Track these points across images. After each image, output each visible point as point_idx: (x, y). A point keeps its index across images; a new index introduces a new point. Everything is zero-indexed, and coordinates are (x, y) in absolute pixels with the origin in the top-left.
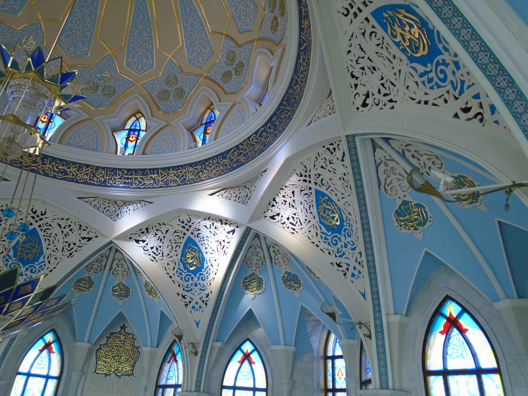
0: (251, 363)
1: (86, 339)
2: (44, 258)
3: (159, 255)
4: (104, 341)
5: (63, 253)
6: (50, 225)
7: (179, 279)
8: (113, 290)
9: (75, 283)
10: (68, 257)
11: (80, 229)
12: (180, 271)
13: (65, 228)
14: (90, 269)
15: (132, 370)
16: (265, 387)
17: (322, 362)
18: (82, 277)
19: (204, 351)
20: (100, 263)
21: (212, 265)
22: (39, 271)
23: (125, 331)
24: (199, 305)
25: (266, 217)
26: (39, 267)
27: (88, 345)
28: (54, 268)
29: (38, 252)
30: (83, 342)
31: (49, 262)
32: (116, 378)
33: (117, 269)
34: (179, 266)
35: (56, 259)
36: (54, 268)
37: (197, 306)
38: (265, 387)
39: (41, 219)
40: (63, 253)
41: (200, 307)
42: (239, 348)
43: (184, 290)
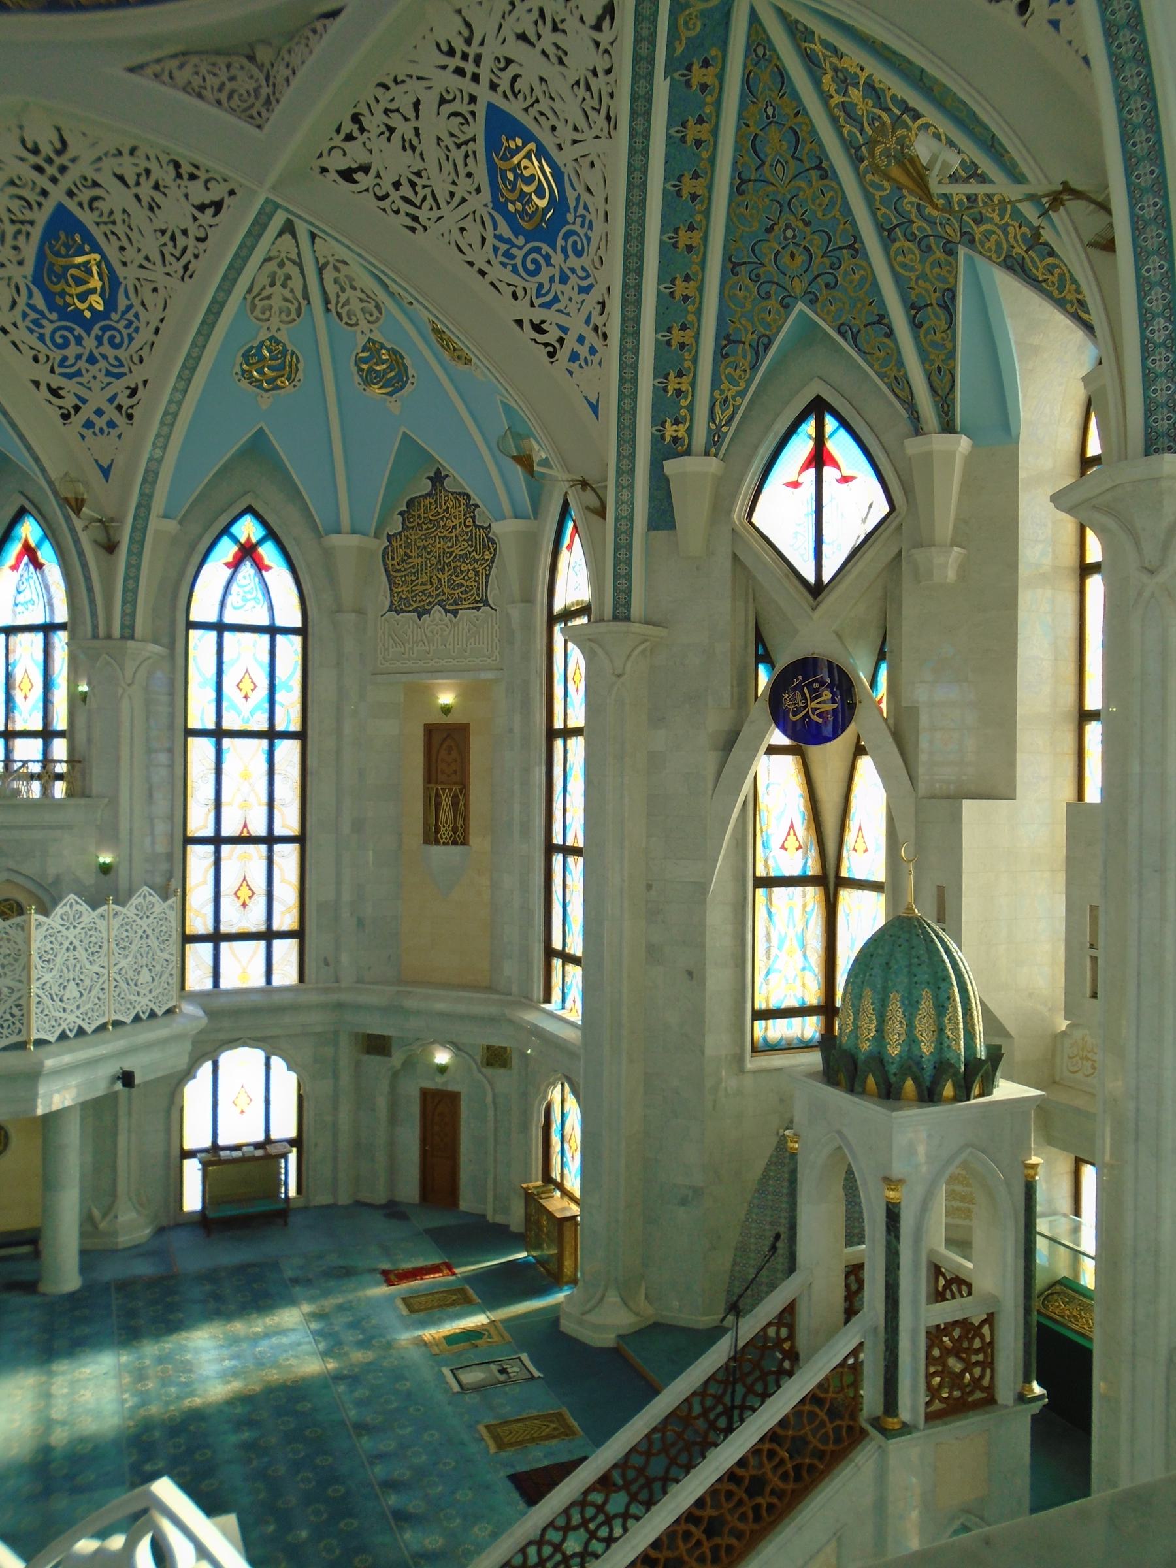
2: (128, 297)
3: (426, 206)
5: (168, 269)
6: (96, 184)
7: (507, 275)
10: (183, 279)
11: (179, 176)
12: (503, 247)
13: (138, 184)
21: (588, 190)
22: (131, 339)
24: (587, 344)
26: (127, 327)
27: (354, 540)
28: (162, 320)
30: (339, 532)
32: (446, 619)
34: (495, 227)
35: (155, 290)
36: (162, 320)
39: (63, 169)
40: (168, 269)
43: (532, 305)
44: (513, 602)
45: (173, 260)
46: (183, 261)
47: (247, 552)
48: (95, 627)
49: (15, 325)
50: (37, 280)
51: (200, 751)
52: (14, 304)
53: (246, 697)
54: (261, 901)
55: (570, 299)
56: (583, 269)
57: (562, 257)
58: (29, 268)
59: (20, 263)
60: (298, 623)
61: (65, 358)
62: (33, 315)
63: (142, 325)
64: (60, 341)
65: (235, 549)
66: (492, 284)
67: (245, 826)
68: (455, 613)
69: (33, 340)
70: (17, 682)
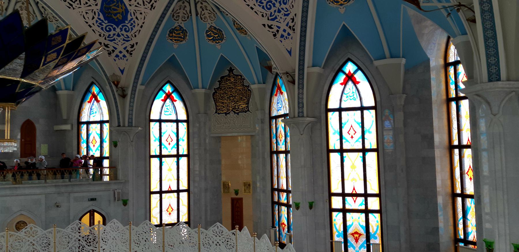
1: (200, 85)
2: (131, 16)
4: (217, 85)
8: (208, 36)
9: (169, 35)
10: (151, 9)
14: (176, 18)
15: (248, 107)
16: (373, 104)
18: (173, 28)
19: (301, 78)
20: (184, 9)
23: (233, 73)
26: (131, 25)
27: (203, 91)
28: (143, 23)
29: (123, 10)
31: (137, 18)
33: (203, 12)
35: (141, 13)
36: (143, 23)
37: (285, 34)
38: (373, 105)
40: (146, 7)
41: (289, 34)
42: (340, 70)
43: (268, 19)
44: (257, 110)
45: (147, 4)
46: (151, 3)
47: (168, 96)
48: (119, 122)
49: (93, 24)
50: (101, 10)
51: (155, 163)
52: (93, 18)
53: (169, 144)
54: (175, 212)
55: (281, 18)
56: (286, 8)
57: (279, 4)
58: (99, 7)
59: (96, 5)
60: (184, 118)
61: (110, 35)
62: (100, 21)
63: (136, 25)
64: (108, 29)
65: (165, 95)
66: (255, 12)
67: (170, 187)
68: (238, 114)
69: (99, 29)
70: (91, 141)
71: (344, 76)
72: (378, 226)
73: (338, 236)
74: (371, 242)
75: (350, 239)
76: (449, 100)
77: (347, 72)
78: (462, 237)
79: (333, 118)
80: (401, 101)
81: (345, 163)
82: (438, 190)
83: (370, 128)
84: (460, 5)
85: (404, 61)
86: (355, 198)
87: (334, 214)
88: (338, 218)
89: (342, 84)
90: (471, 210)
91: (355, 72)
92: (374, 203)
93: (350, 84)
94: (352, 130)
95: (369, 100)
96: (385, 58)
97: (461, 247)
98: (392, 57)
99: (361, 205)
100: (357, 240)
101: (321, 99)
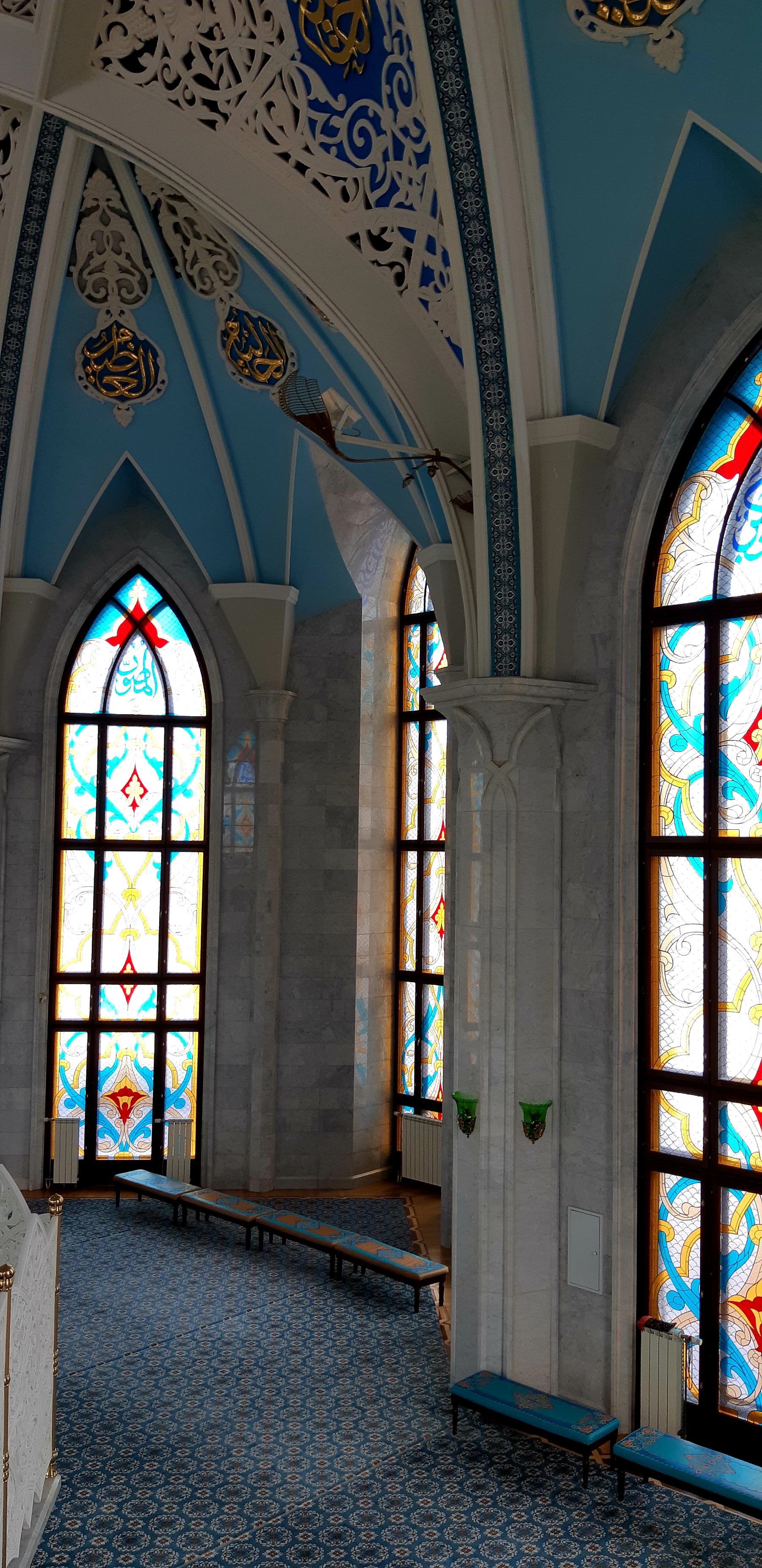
0: (154, 643)
16: (202, 712)
17: (393, 637)
25: (107, 61)
38: (202, 712)
42: (110, 598)
71: (122, 619)
72: (189, 1070)
73: (69, 1104)
74: (168, 1116)
75: (107, 1111)
76: (403, 718)
77: (131, 607)
78: (411, 1090)
79: (80, 742)
80: (277, 709)
81: (107, 884)
82: (359, 961)
83: (189, 780)
84: (437, 457)
85: (292, 595)
86: (128, 987)
87: (63, 1037)
88: (71, 1049)
89: (112, 641)
90: (436, 1018)
91: (155, 609)
92: (183, 1002)
93: (138, 645)
94: (135, 784)
95: (191, 701)
96: (242, 579)
97: (407, 1117)
98: (262, 579)
99: (145, 1007)
100: (125, 1114)
101: (45, 681)
